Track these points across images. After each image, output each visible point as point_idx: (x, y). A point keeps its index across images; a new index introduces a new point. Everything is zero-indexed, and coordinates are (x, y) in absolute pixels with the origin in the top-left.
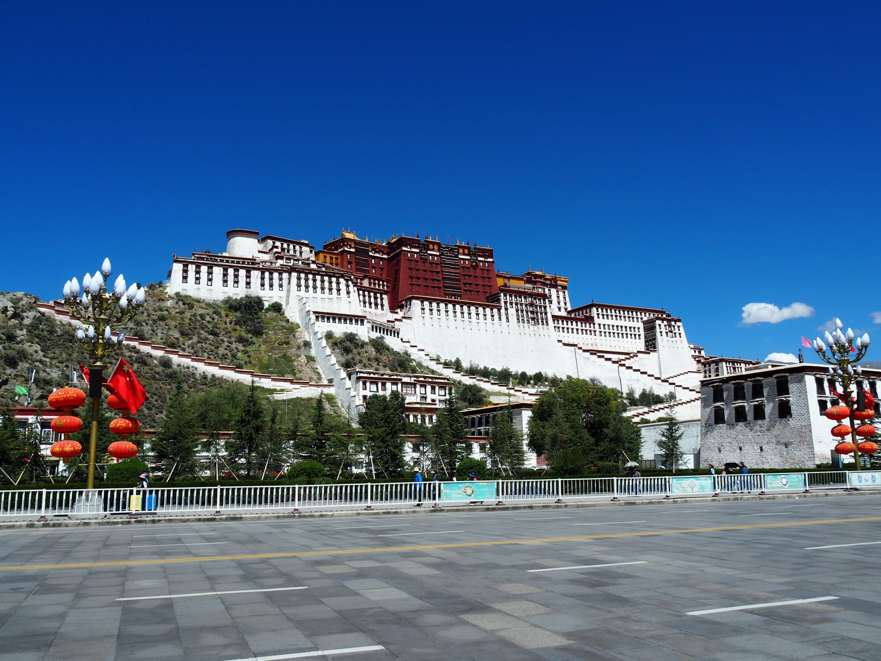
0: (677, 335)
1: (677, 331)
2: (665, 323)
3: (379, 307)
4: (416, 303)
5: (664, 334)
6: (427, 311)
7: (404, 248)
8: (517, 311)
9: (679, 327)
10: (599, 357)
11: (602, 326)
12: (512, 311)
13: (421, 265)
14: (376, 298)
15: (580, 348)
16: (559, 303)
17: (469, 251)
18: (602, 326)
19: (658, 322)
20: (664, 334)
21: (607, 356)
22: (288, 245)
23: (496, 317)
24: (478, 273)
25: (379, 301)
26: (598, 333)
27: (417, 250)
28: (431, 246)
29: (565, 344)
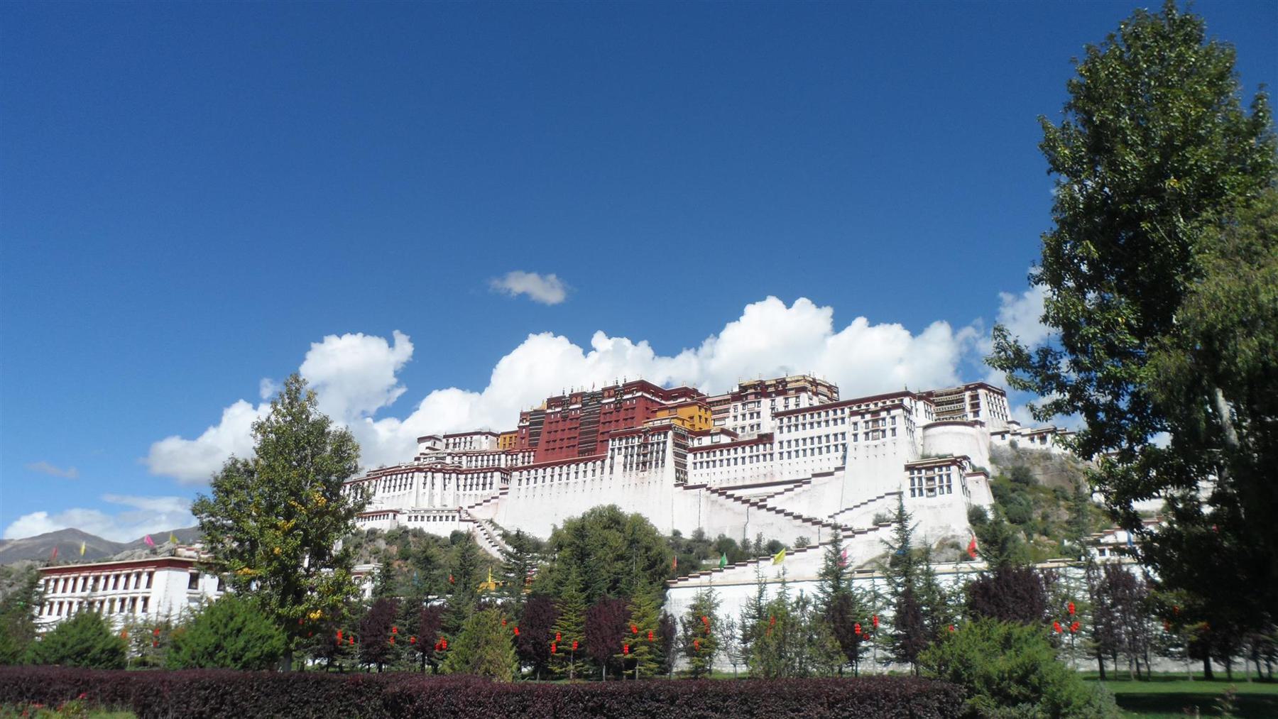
0: (889, 433)
1: (888, 426)
2: (868, 417)
5: (861, 437)
8: (626, 457)
9: (893, 418)
11: (785, 444)
12: (619, 459)
13: (561, 426)
14: (485, 478)
18: (785, 444)
20: (861, 437)
21: (737, 493)
23: (598, 471)
24: (622, 415)
25: (488, 480)
26: (777, 456)
29: (687, 488)
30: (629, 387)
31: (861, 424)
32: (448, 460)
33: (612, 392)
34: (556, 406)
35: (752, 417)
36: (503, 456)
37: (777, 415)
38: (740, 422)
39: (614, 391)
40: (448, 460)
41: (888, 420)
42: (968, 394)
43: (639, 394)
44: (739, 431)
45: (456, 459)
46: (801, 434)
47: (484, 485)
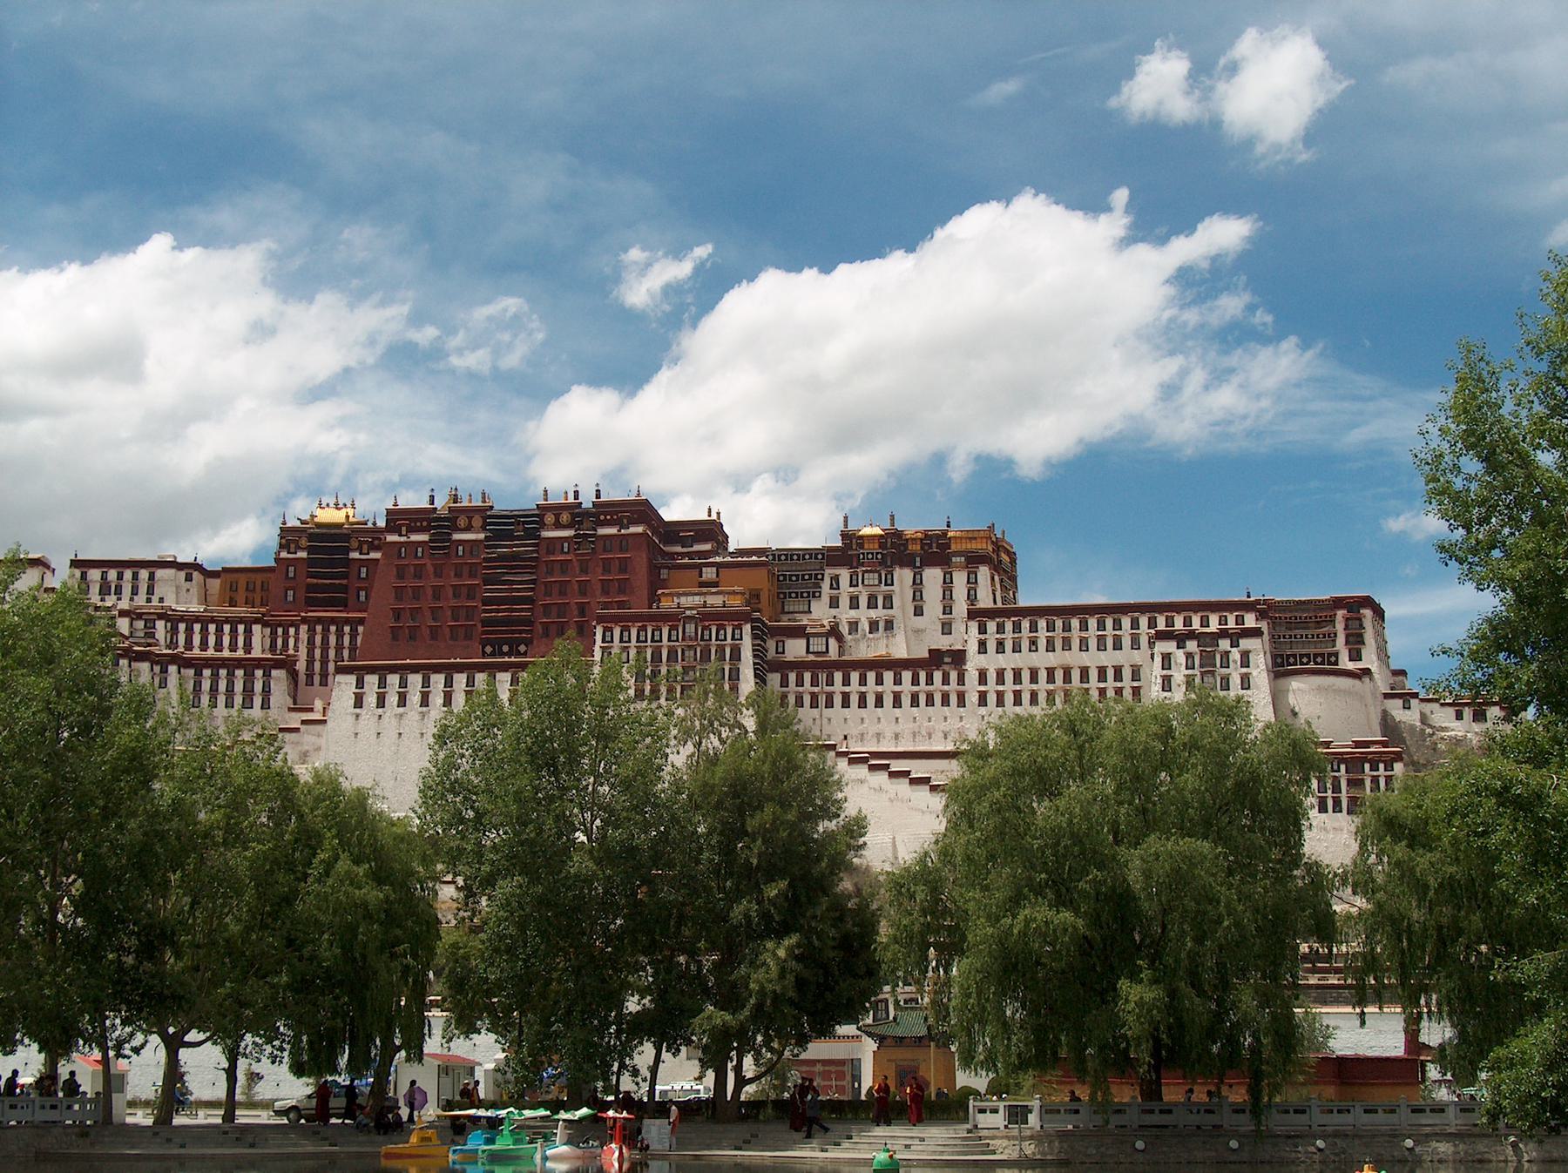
2: (1192, 646)
3: (258, 701)
4: (344, 686)
6: (370, 699)
7: (391, 538)
10: (894, 775)
11: (992, 677)
15: (845, 754)
16: (947, 610)
17: (574, 516)
18: (992, 677)
19: (1163, 647)
22: (120, 577)
25: (258, 686)
26: (972, 698)
27: (424, 537)
28: (462, 522)
30: (608, 511)
31: (1180, 657)
32: (123, 625)
33: (565, 517)
34: (411, 530)
35: (872, 604)
36: (256, 628)
37: (972, 615)
38: (845, 614)
39: (572, 513)
40: (123, 625)
41: (1235, 655)
42: (1341, 613)
43: (639, 529)
44: (844, 629)
45: (140, 624)
46: (1025, 660)
47: (248, 692)
